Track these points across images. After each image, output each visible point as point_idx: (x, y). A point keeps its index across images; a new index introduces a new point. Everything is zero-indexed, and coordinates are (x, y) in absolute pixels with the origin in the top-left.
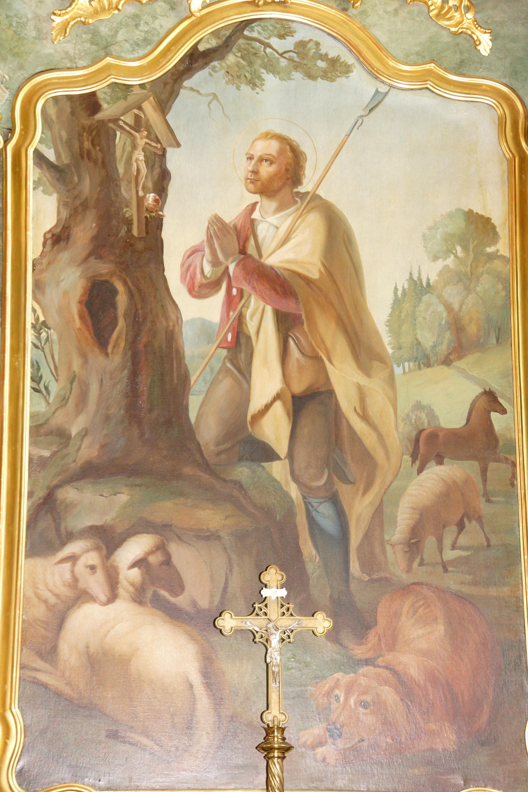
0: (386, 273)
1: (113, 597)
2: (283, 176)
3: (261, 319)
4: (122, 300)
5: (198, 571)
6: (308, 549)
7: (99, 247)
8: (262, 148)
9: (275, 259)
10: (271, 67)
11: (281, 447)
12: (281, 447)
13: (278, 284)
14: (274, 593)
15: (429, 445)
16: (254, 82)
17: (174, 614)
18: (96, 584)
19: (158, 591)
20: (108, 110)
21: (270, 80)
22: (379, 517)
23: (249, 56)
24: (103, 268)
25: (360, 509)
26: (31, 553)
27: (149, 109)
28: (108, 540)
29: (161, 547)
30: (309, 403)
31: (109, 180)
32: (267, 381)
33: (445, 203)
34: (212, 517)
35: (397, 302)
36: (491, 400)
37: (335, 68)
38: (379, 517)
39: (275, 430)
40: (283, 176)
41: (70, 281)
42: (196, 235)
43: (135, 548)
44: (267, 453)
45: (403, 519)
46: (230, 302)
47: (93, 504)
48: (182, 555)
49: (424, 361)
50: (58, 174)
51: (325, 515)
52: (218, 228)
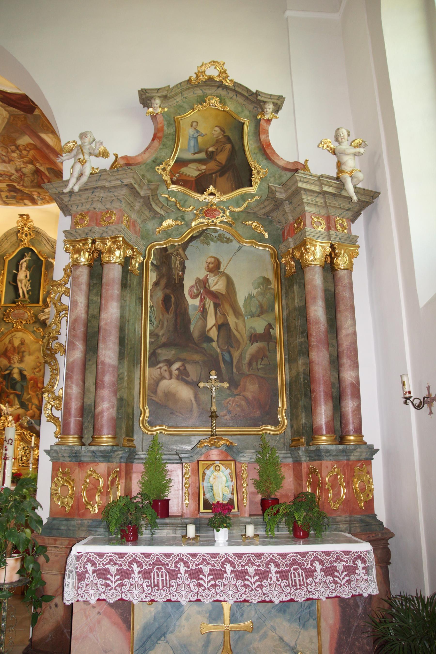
0: (242, 293)
1: (171, 378)
2: (215, 267)
3: (210, 305)
4: (173, 300)
5: (193, 372)
6: (222, 365)
7: (167, 286)
8: (210, 260)
9: (213, 289)
10: (212, 240)
11: (215, 339)
12: (215, 339)
13: (214, 295)
14: (213, 377)
15: (254, 338)
16: (208, 244)
17: (187, 383)
18: (166, 375)
19: (183, 376)
20: (170, 251)
21: (212, 243)
22: (241, 357)
23: (206, 237)
24: (168, 291)
25: (236, 355)
26: (149, 366)
27: (180, 251)
28: (169, 363)
29: (183, 365)
30: (223, 327)
31: (170, 269)
32: (211, 321)
33: (257, 275)
34: (197, 357)
35: (246, 300)
36: (270, 326)
37: (229, 240)
38: (241, 357)
39: (213, 334)
40: (215, 267)
41: (160, 295)
42: (192, 283)
43: (176, 365)
45: (247, 357)
46: (201, 300)
47: (166, 354)
48: (189, 368)
50: (156, 267)
51: (227, 356)
52: (198, 280)
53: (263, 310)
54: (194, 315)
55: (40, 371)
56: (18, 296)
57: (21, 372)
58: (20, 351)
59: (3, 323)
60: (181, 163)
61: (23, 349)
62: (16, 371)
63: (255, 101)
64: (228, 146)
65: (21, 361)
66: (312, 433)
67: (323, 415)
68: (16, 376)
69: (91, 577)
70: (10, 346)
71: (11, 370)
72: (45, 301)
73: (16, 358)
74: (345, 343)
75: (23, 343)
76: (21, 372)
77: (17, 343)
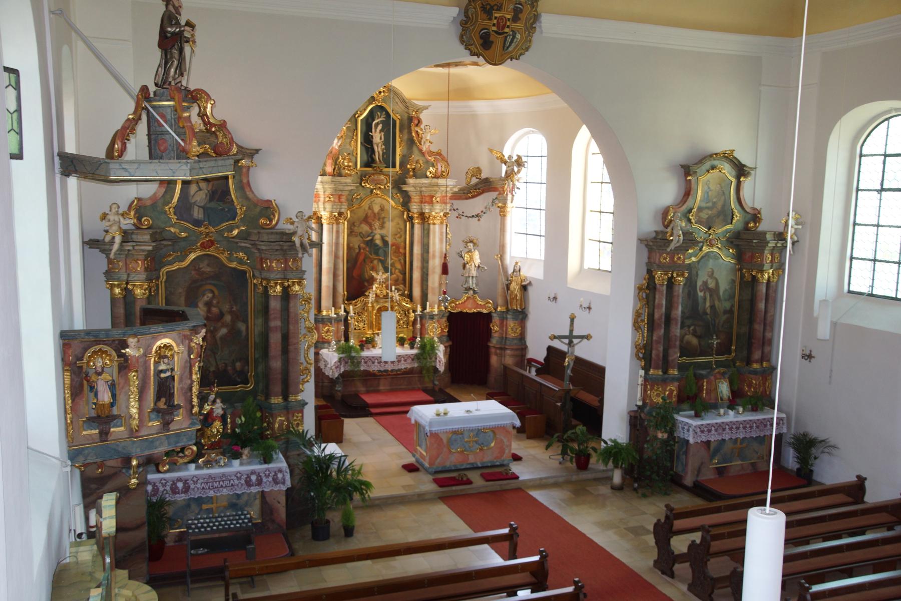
2: (711, 275)
13: (710, 290)
15: (725, 312)
17: (696, 336)
19: (694, 334)
25: (717, 321)
28: (689, 327)
30: (712, 307)
32: (708, 304)
36: (733, 306)
39: (708, 311)
41: (686, 291)
43: (692, 328)
44: (707, 314)
47: (688, 322)
49: (725, 300)
53: (732, 297)
54: (700, 300)
55: (400, 237)
56: (373, 161)
57: (383, 238)
58: (380, 217)
59: (361, 188)
60: (700, 209)
61: (383, 215)
62: (378, 237)
63: (741, 171)
64: (723, 198)
65: (382, 227)
66: (749, 362)
67: (757, 355)
68: (378, 242)
69: (699, 433)
70: (370, 212)
71: (373, 237)
72: (402, 165)
73: (377, 224)
74: (769, 319)
75: (382, 209)
76: (383, 238)
77: (376, 209)
